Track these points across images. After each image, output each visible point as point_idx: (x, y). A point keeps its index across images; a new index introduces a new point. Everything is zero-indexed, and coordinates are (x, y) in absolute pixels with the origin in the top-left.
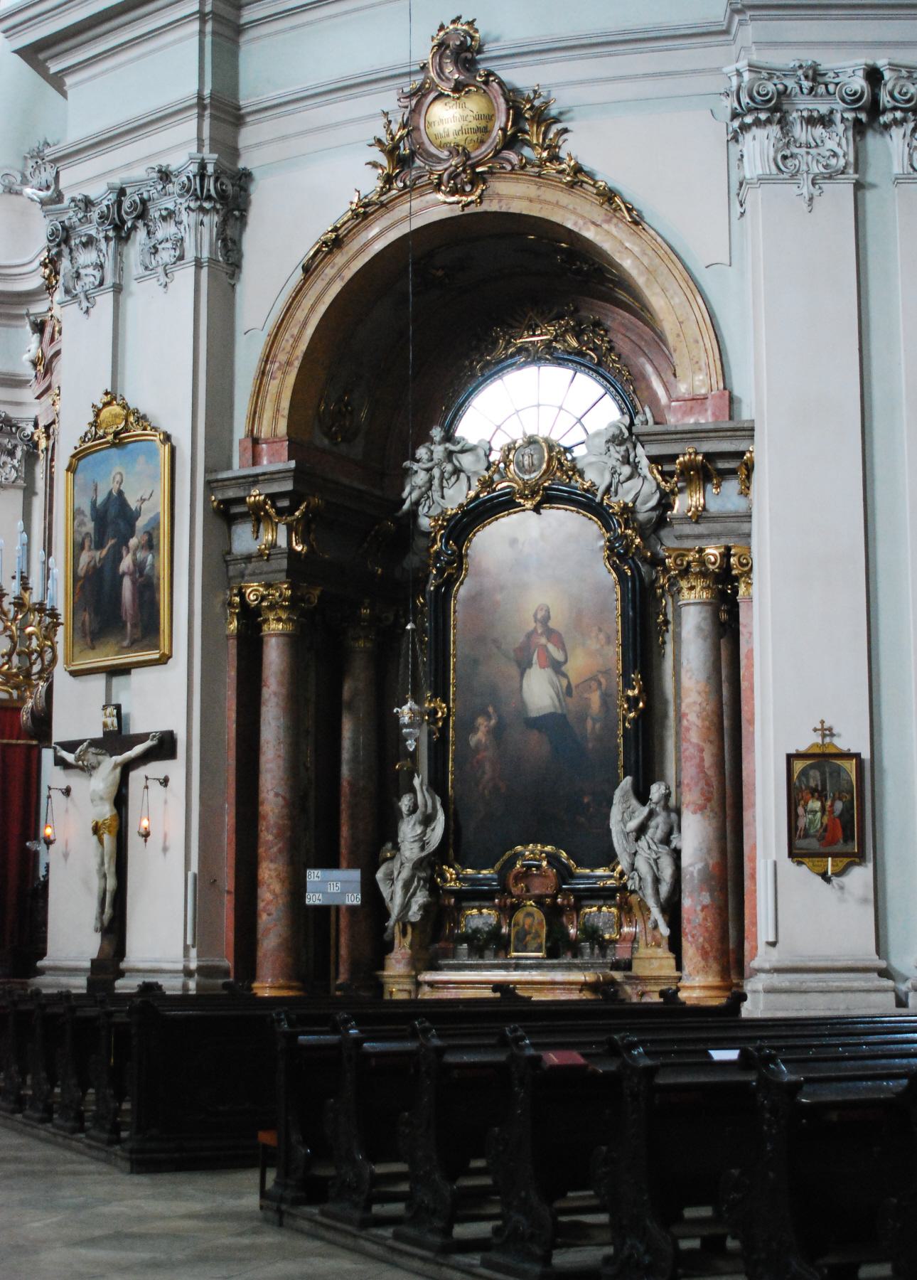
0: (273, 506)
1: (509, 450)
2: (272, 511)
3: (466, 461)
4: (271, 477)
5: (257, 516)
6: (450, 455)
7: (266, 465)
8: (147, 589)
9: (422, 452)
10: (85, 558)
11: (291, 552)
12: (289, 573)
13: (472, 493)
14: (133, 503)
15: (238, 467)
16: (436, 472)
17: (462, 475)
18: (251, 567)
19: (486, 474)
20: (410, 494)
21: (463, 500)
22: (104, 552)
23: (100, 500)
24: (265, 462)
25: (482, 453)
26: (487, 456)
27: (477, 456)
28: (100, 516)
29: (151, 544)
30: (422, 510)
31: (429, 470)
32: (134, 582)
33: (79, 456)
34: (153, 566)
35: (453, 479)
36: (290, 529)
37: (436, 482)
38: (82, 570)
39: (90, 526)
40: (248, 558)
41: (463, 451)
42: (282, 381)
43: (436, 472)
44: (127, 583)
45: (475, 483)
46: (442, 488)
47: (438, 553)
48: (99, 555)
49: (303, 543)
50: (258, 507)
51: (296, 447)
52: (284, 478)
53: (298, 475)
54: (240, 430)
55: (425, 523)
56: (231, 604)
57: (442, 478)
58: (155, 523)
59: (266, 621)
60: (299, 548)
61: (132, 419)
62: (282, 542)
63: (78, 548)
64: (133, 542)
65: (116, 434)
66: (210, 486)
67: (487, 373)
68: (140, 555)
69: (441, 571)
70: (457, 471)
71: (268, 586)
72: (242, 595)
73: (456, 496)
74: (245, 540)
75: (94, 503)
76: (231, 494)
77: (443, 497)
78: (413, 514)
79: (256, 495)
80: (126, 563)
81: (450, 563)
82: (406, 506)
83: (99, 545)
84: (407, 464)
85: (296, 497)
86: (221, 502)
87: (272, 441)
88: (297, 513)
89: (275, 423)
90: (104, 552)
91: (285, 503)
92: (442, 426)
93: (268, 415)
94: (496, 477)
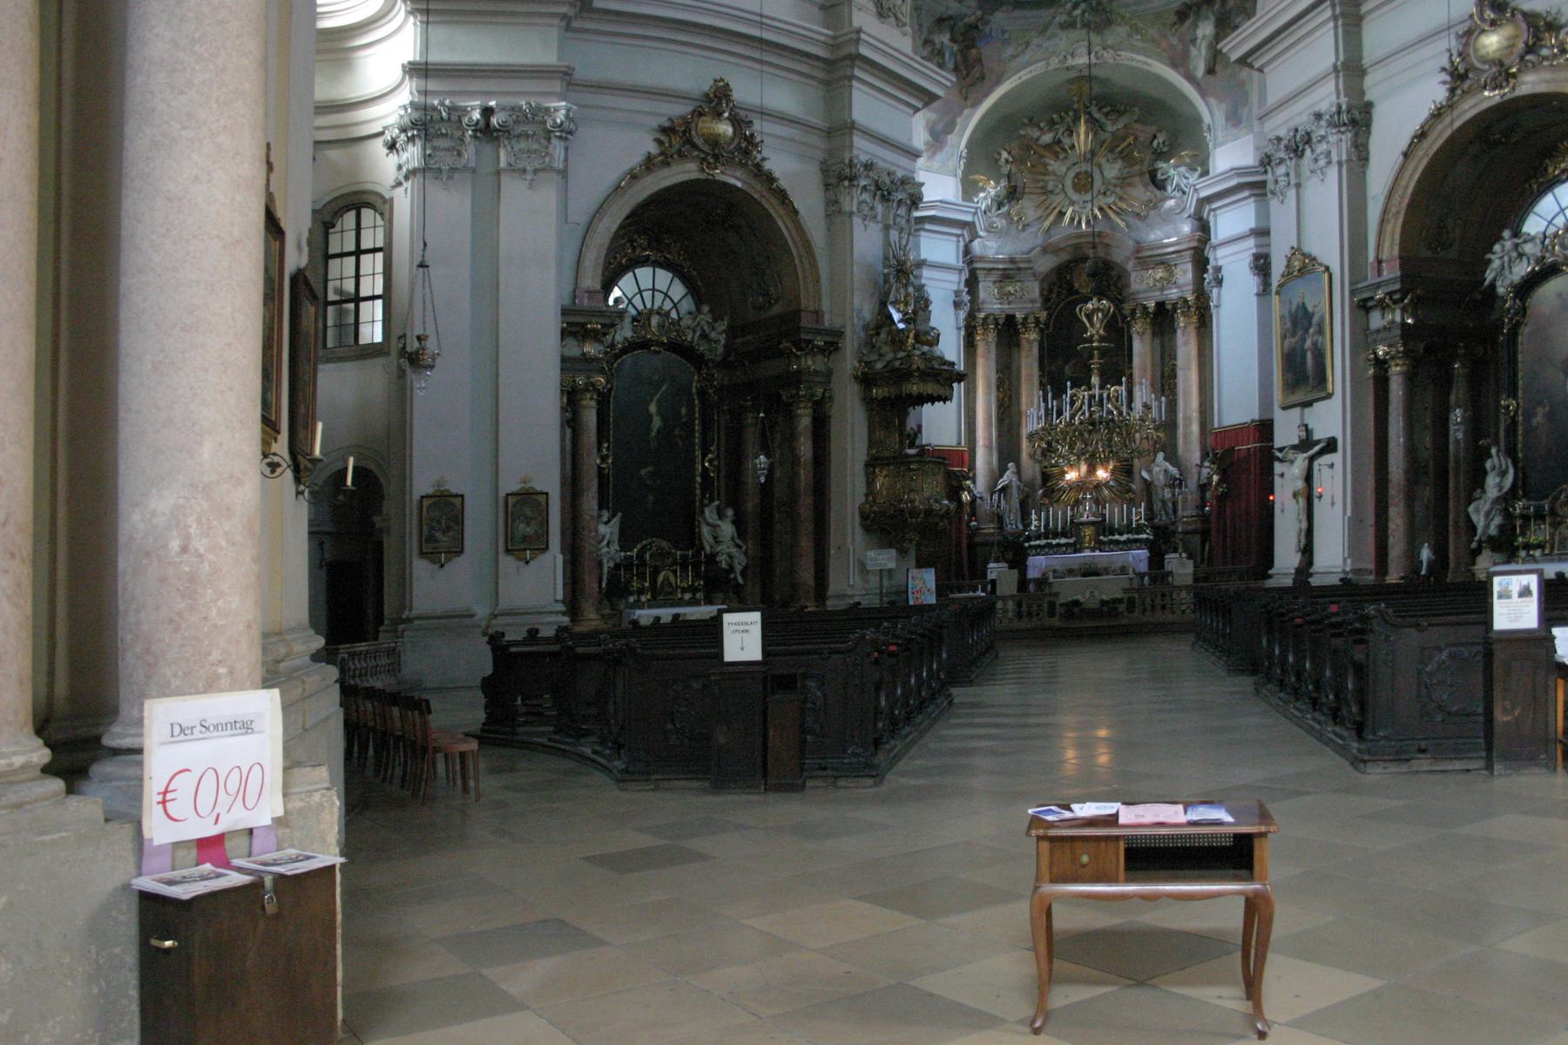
0: (1391, 299)
1: (1555, 237)
2: (1390, 303)
3: (1528, 248)
4: (1387, 282)
5: (1382, 306)
6: (1516, 246)
7: (1386, 275)
8: (1319, 356)
9: (1497, 247)
10: (1287, 342)
11: (1404, 324)
12: (1402, 336)
13: (1529, 269)
14: (1310, 309)
15: (1372, 278)
16: (1506, 259)
17: (1525, 259)
18: (1380, 336)
19: (1539, 254)
20: (1489, 276)
21: (1523, 273)
22: (1297, 338)
23: (1294, 307)
24: (1385, 273)
25: (1538, 241)
26: (1543, 243)
27: (1536, 244)
28: (1295, 321)
29: (1320, 331)
30: (1499, 283)
31: (1501, 258)
32: (1313, 353)
33: (1280, 286)
34: (1322, 344)
35: (1518, 261)
36: (1404, 310)
37: (1506, 265)
38: (1286, 350)
39: (1289, 325)
40: (1378, 331)
41: (1525, 242)
42: (1395, 223)
43: (1506, 259)
44: (1309, 355)
45: (1532, 262)
46: (1510, 268)
47: (1509, 310)
48: (1294, 340)
49: (1413, 316)
50: (1382, 301)
51: (1405, 260)
52: (1394, 283)
53: (1404, 278)
54: (1371, 257)
55: (1501, 290)
56: (1369, 360)
57: (1510, 261)
58: (1322, 319)
59: (1389, 367)
60: (1410, 321)
61: (1307, 261)
62: (1398, 319)
63: (1284, 337)
64: (1311, 331)
65: (1299, 270)
66: (1353, 293)
67: (1541, 189)
68: (1315, 338)
69: (1511, 319)
70: (1521, 255)
71: (1390, 346)
72: (1375, 353)
73: (1522, 270)
74: (1376, 320)
75: (1290, 311)
76: (1365, 296)
77: (1511, 273)
78: (1493, 286)
79: (1379, 295)
80: (1308, 343)
81: (1516, 314)
82: (1487, 283)
83: (1294, 334)
84: (1488, 256)
85: (1404, 292)
86: (1360, 301)
87: (1388, 261)
88: (1406, 301)
89: (1392, 250)
90: (1297, 338)
91: (1397, 296)
92: (1512, 229)
93: (1387, 244)
94: (1547, 255)
